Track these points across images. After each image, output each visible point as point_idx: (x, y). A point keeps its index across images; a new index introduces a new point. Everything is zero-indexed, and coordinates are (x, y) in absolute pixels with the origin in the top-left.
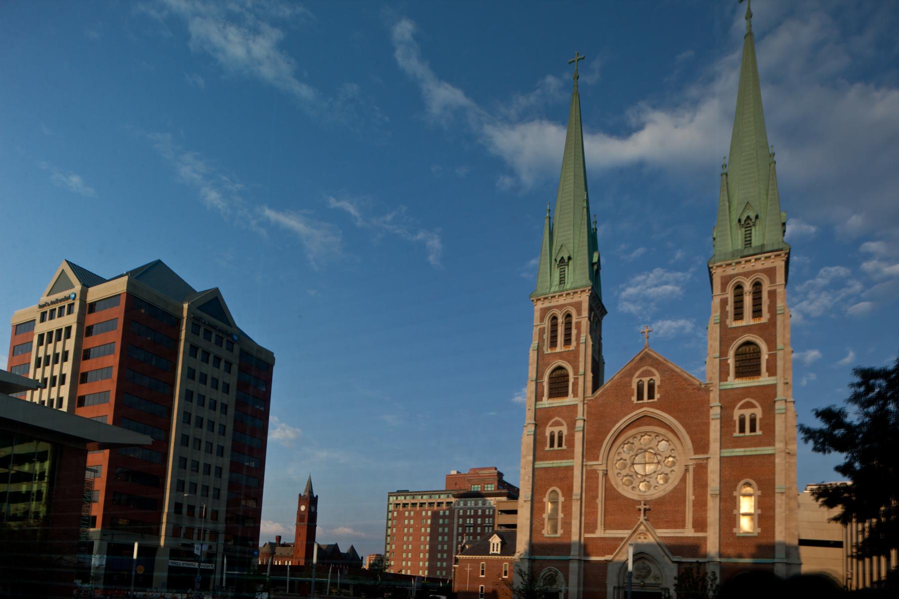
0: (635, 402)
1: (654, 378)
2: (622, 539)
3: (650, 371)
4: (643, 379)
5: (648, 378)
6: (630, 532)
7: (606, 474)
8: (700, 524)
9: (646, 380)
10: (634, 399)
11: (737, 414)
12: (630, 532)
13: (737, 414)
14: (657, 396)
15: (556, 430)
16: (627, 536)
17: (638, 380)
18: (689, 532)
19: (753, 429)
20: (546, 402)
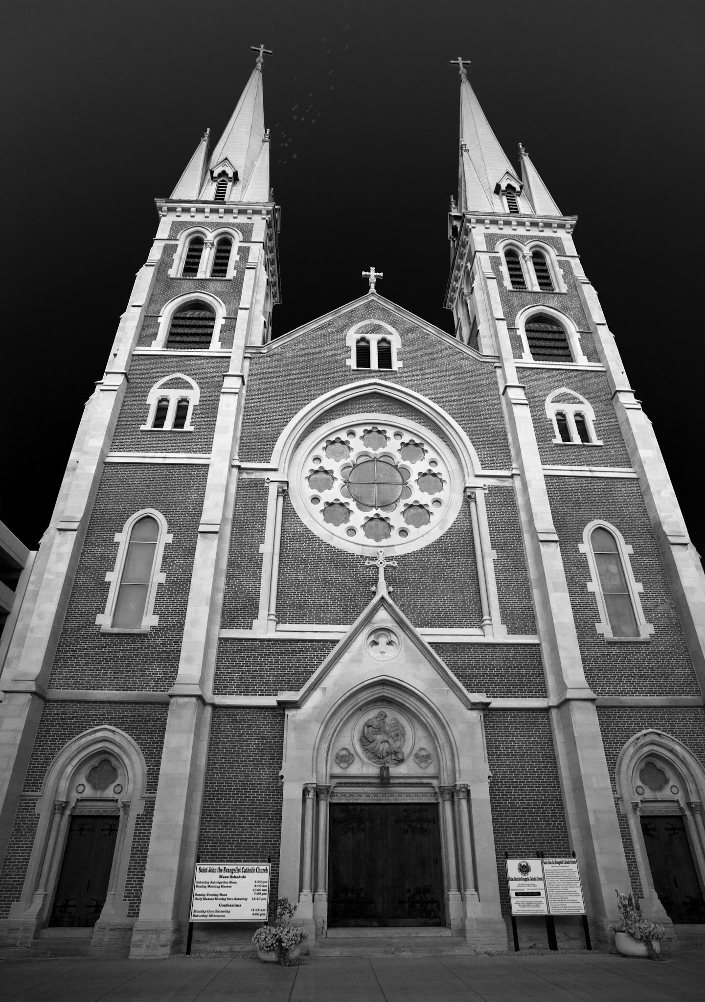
0: (354, 367)
1: (388, 337)
2: (335, 642)
3: (380, 327)
4: (368, 336)
5: (379, 337)
6: (348, 629)
7: (284, 493)
8: (521, 612)
9: (374, 340)
10: (352, 362)
11: (551, 411)
12: (348, 629)
13: (551, 411)
14: (396, 364)
15: (174, 396)
16: (342, 638)
17: (359, 336)
18: (496, 633)
19: (584, 436)
20: (157, 347)
